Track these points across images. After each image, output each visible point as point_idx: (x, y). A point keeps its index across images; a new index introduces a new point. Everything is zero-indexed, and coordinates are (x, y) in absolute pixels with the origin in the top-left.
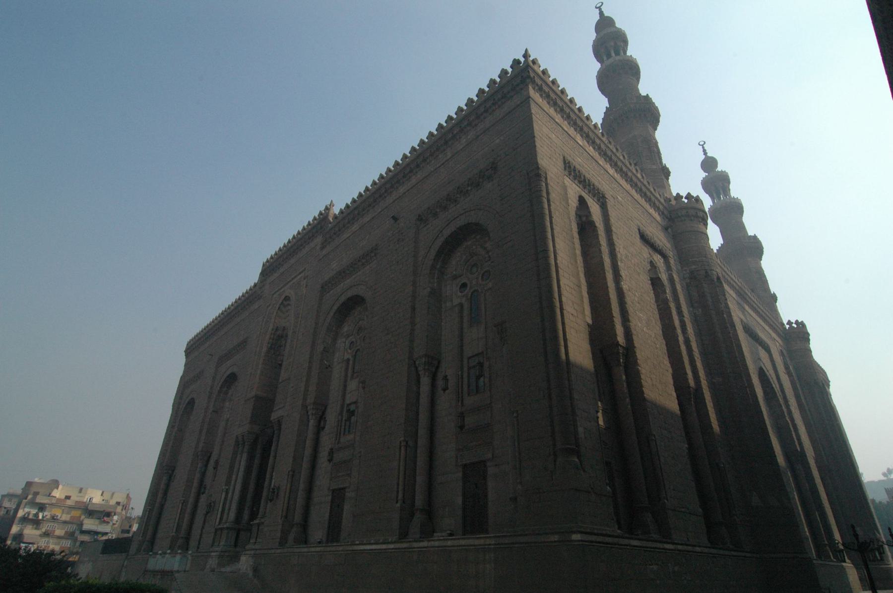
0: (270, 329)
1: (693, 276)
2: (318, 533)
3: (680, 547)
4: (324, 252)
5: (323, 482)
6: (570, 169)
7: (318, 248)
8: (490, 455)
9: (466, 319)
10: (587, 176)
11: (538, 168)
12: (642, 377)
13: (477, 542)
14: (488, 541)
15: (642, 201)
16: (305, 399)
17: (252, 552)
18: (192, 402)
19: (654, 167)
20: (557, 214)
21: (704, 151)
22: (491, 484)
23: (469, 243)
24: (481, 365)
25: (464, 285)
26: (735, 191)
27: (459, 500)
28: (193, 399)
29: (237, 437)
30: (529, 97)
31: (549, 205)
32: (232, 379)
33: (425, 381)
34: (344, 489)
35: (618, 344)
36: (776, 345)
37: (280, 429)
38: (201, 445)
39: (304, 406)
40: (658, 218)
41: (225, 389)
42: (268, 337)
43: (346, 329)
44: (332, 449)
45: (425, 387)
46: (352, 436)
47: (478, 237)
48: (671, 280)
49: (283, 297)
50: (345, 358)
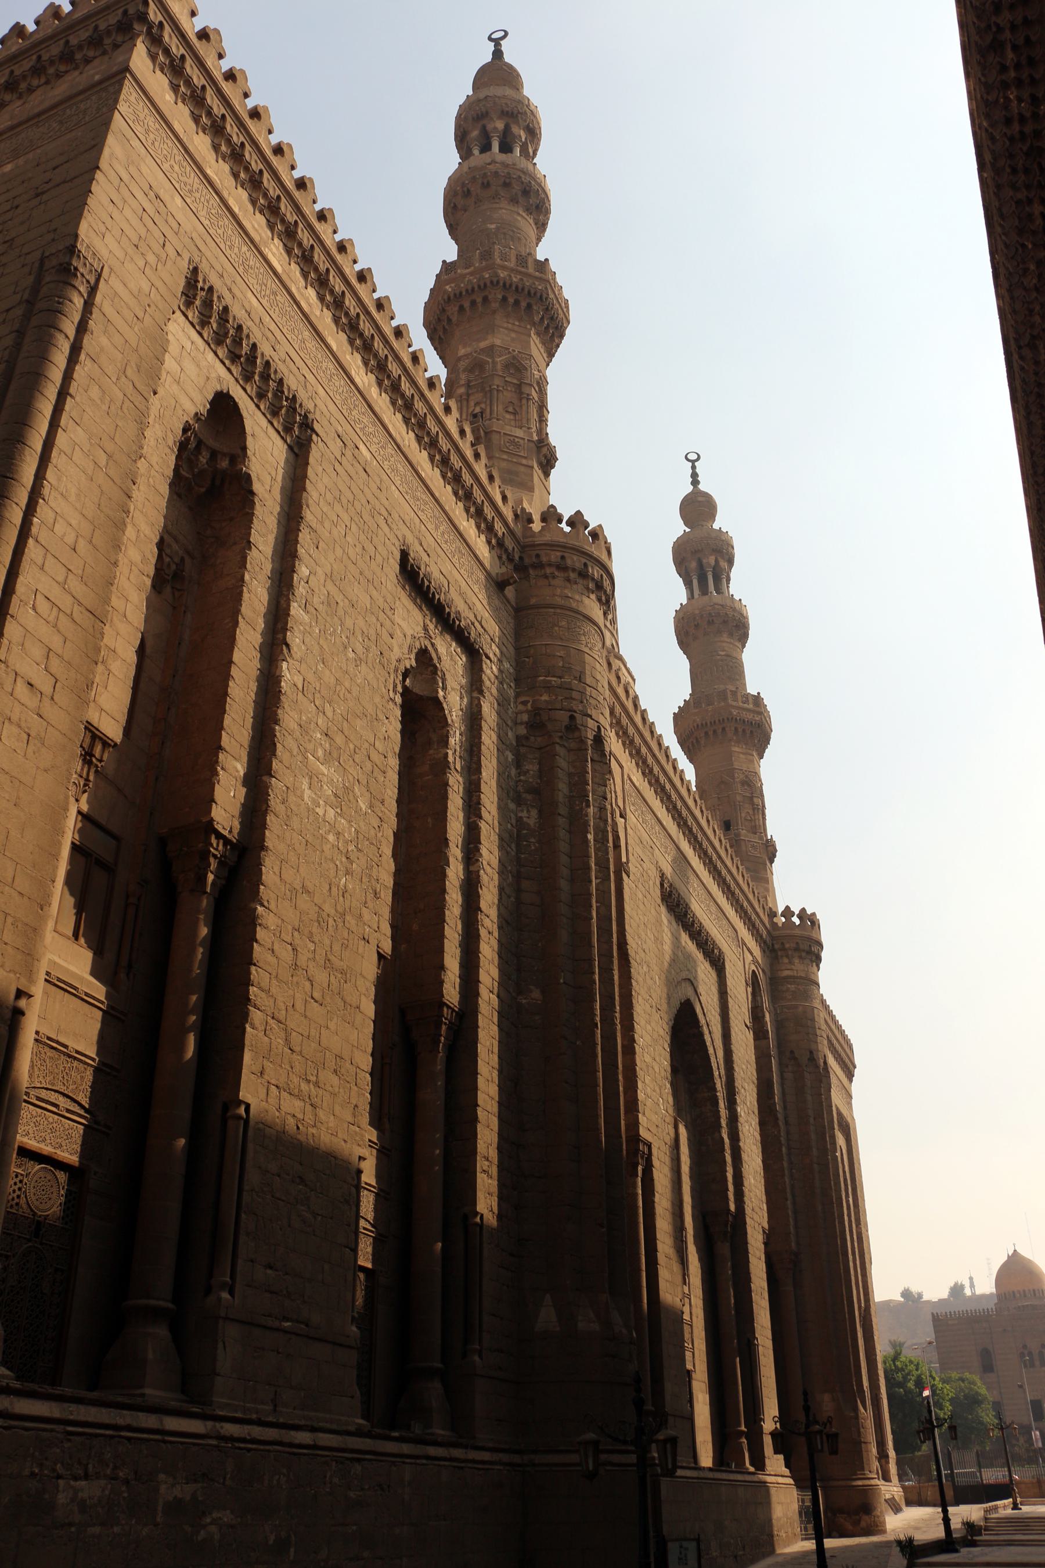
1: (537, 723)
3: (231, 1429)
6: (198, 297)
10: (265, 349)
11: (72, 250)
12: (260, 934)
15: (445, 493)
19: (519, 433)
20: (95, 392)
21: (694, 476)
26: (740, 585)
30: (127, 69)
31: (73, 359)
35: (209, 828)
36: (742, 958)
40: (483, 550)
48: (473, 719)
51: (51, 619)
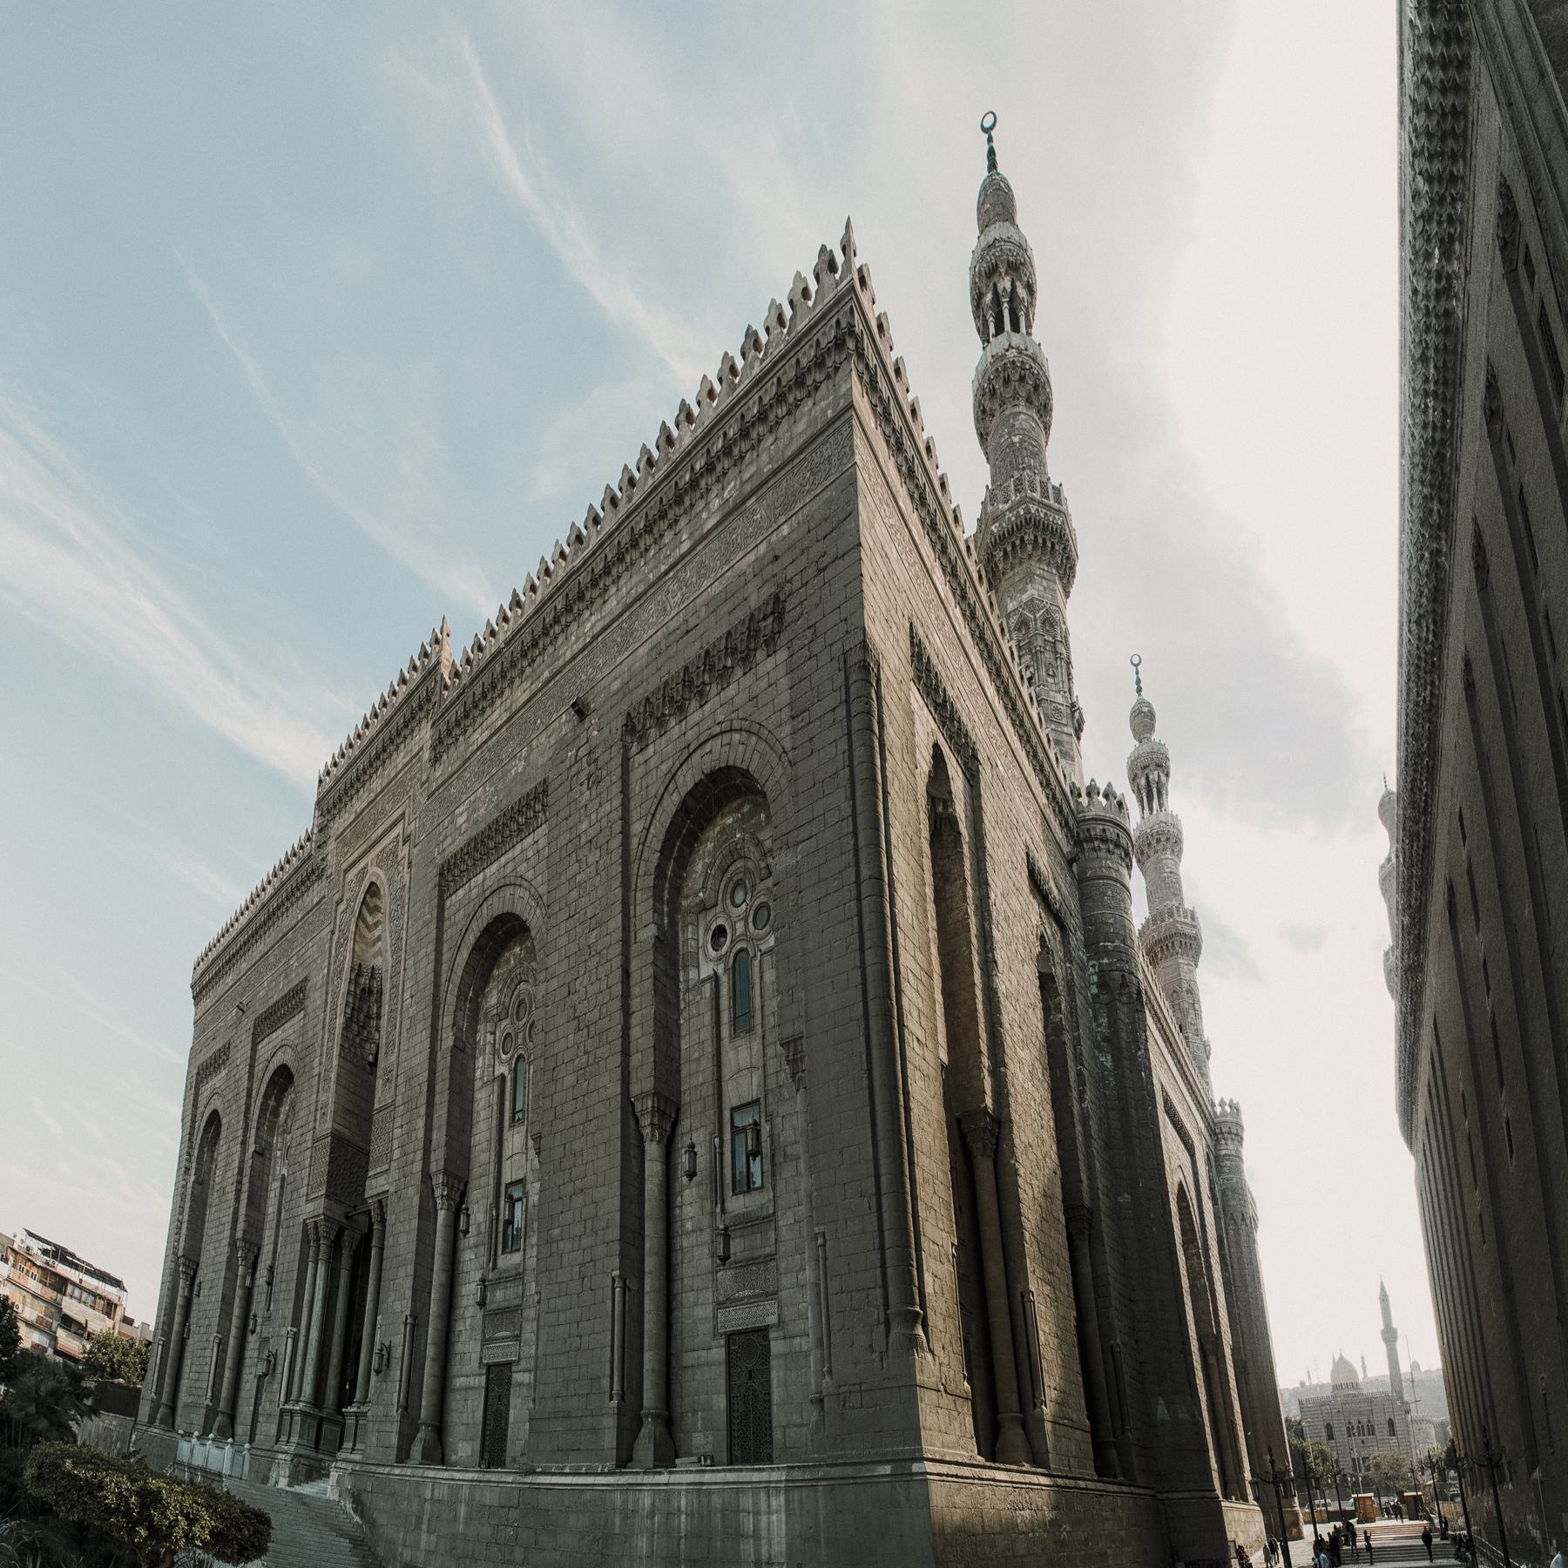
0: (347, 965)
2: (464, 1446)
5: (470, 1350)
13: (756, 1477)
14: (775, 1476)
16: (426, 1160)
17: (350, 1467)
18: (215, 1118)
28: (215, 1112)
29: (305, 1225)
32: (283, 1079)
33: (652, 1150)
37: (383, 1221)
38: (241, 1226)
39: (426, 1176)
42: (344, 987)
44: (483, 1281)
45: (653, 1168)
46: (516, 1258)
49: (366, 884)
50: (497, 1073)
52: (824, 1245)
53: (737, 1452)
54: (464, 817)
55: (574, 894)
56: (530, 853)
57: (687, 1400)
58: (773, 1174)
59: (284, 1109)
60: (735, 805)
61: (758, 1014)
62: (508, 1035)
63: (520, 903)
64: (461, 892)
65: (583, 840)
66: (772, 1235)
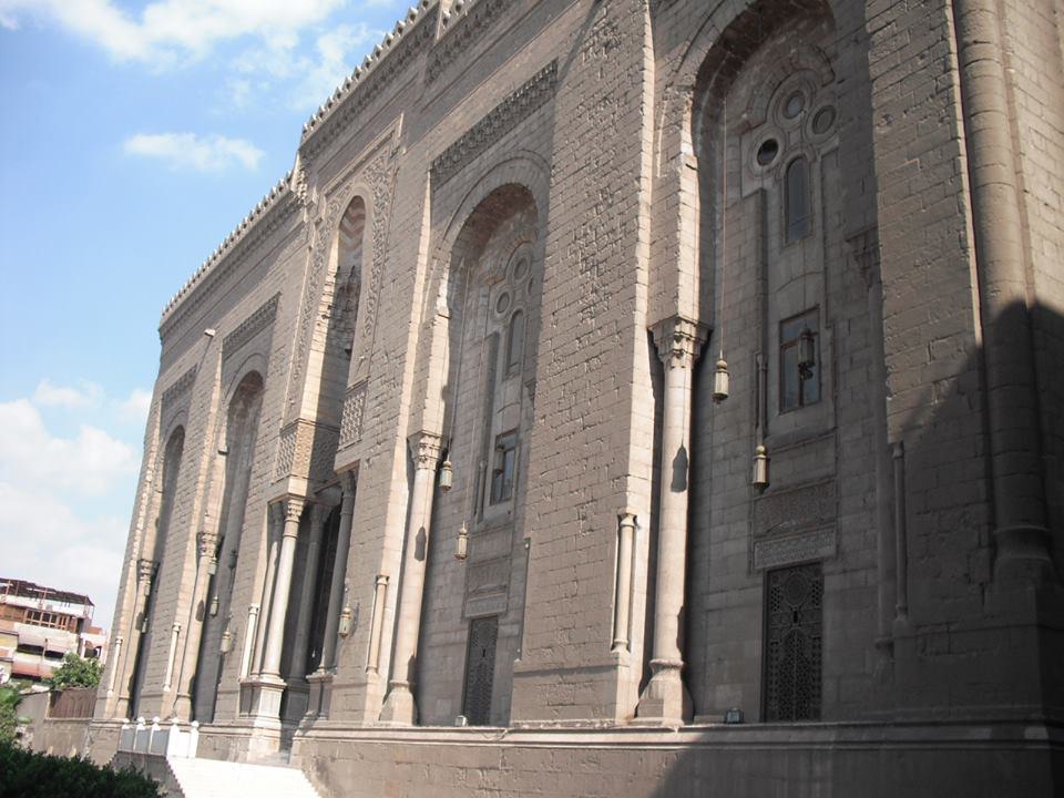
4: (435, 88)
7: (421, 80)
8: (828, 550)
9: (774, 228)
13: (795, 736)
14: (821, 736)
22: (830, 614)
23: (783, 39)
24: (809, 336)
25: (769, 147)
27: (754, 648)
34: (495, 617)
37: (354, 489)
41: (240, 406)
43: (488, 263)
47: (801, 26)
50: (489, 333)
51: (1043, 148)
52: (902, 457)
53: (774, 706)
54: (461, 115)
55: (584, 149)
56: (535, 127)
57: (711, 649)
58: (835, 384)
59: (251, 411)
60: (787, 25)
61: (818, 220)
62: (505, 295)
63: (519, 174)
64: (454, 180)
65: (598, 97)
66: (830, 453)
